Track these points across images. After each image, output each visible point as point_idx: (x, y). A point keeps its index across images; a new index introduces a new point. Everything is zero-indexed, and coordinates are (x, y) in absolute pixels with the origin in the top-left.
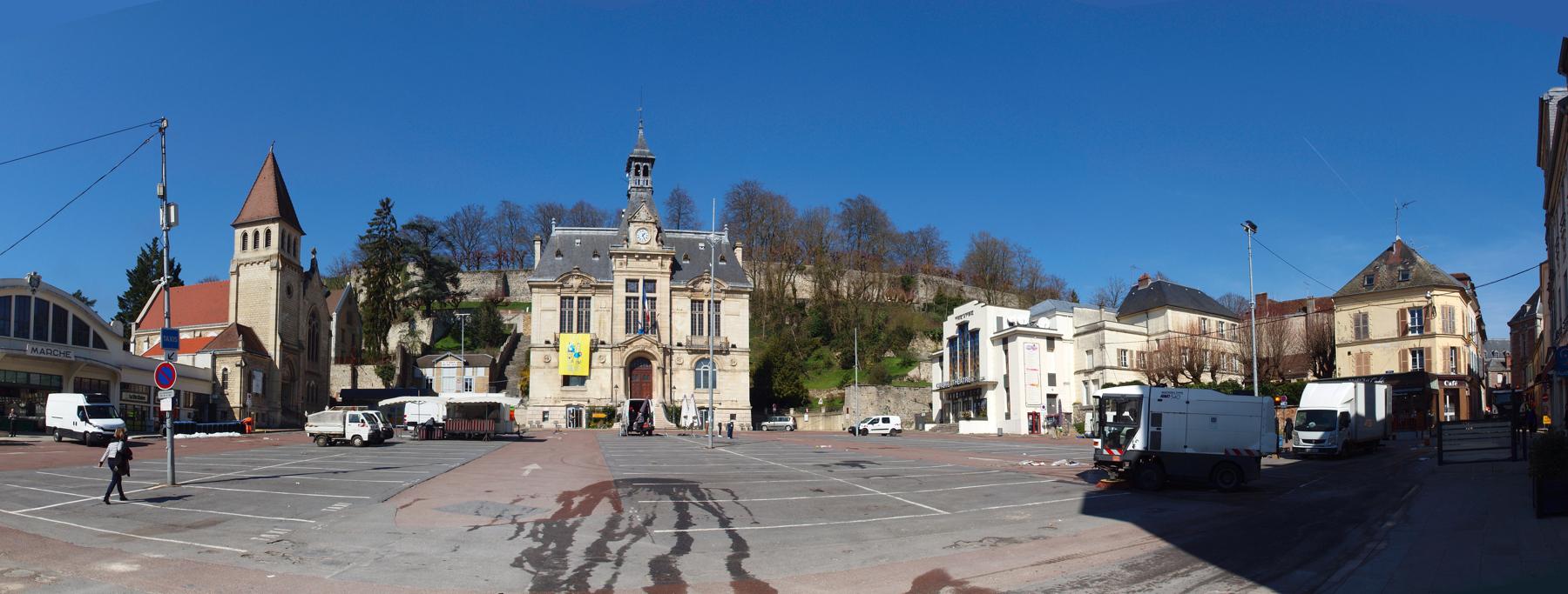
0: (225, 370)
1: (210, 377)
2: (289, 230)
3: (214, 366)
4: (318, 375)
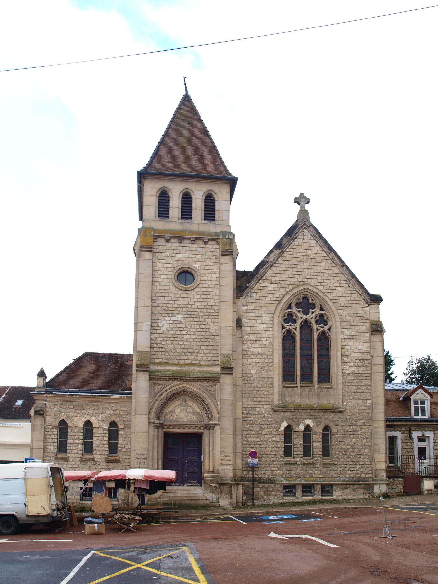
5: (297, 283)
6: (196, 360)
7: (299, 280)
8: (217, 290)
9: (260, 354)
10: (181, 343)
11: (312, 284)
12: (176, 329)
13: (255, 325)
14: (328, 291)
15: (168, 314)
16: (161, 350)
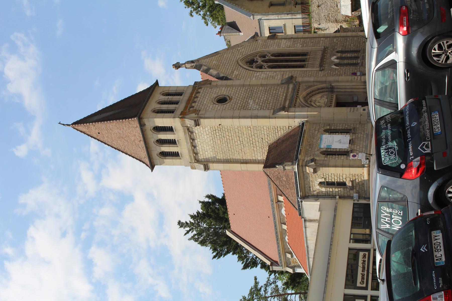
0: (321, 183)
1: (329, 203)
2: (153, 104)
3: (317, 197)
4: (325, 51)
5: (236, 64)
6: (283, 95)
7: (234, 63)
8: (234, 88)
14: (244, 53)
15: (247, 106)
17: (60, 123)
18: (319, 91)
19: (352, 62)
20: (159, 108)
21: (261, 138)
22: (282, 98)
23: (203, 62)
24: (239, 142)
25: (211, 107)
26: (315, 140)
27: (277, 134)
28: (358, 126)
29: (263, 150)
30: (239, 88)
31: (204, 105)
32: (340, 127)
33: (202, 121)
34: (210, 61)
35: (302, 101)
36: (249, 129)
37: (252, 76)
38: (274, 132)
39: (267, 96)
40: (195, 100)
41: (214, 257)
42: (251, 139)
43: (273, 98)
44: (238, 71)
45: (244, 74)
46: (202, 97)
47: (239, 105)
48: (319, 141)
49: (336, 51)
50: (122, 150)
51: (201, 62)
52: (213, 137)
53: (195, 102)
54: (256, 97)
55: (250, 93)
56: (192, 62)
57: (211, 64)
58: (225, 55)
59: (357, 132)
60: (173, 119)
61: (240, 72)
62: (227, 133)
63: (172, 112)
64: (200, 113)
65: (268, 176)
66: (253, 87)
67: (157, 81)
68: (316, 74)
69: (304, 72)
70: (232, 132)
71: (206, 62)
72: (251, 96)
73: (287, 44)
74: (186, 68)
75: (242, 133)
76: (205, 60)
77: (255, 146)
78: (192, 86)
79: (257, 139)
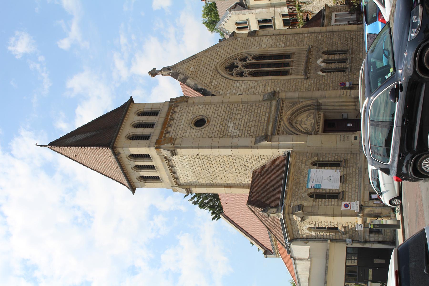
0: (310, 229)
1: (320, 245)
3: (307, 240)
4: (309, 51)
5: (214, 71)
6: (266, 115)
7: (212, 69)
8: (213, 106)
9: (265, 87)
10: (251, 123)
11: (216, 64)
12: (239, 126)
13: (242, 89)
14: (223, 56)
15: (227, 130)
16: (255, 133)
17: (36, 145)
18: (305, 109)
19: (340, 67)
20: (134, 133)
21: (244, 165)
22: (265, 119)
23: (180, 69)
24: (220, 168)
25: (188, 133)
26: (302, 177)
27: (261, 161)
28: (349, 157)
29: (247, 176)
30: (218, 106)
31: (181, 129)
32: (329, 158)
33: (179, 151)
34: (187, 67)
35: (286, 123)
36: (230, 157)
37: (232, 87)
38: (258, 160)
39: (248, 116)
40: (172, 122)
41: (214, 218)
42: (233, 166)
43: (254, 119)
44: (217, 80)
45: (223, 84)
46: (178, 119)
47: (218, 129)
48: (306, 179)
49: (322, 51)
50: (101, 171)
51: (178, 69)
52: (193, 164)
53: (171, 125)
54: (236, 118)
55: (229, 113)
56: (168, 69)
57: (188, 71)
58: (203, 59)
59: (349, 165)
60: (148, 148)
61: (219, 81)
62: (207, 161)
63: (146, 138)
64: (177, 141)
65: (253, 212)
66: (233, 104)
67: (131, 97)
68: (301, 83)
69: (288, 81)
70: (212, 160)
71: (183, 68)
72: (231, 116)
73: (269, 42)
74: (163, 75)
75: (223, 160)
76: (182, 66)
77: (238, 172)
78: (168, 104)
79: (239, 166)
